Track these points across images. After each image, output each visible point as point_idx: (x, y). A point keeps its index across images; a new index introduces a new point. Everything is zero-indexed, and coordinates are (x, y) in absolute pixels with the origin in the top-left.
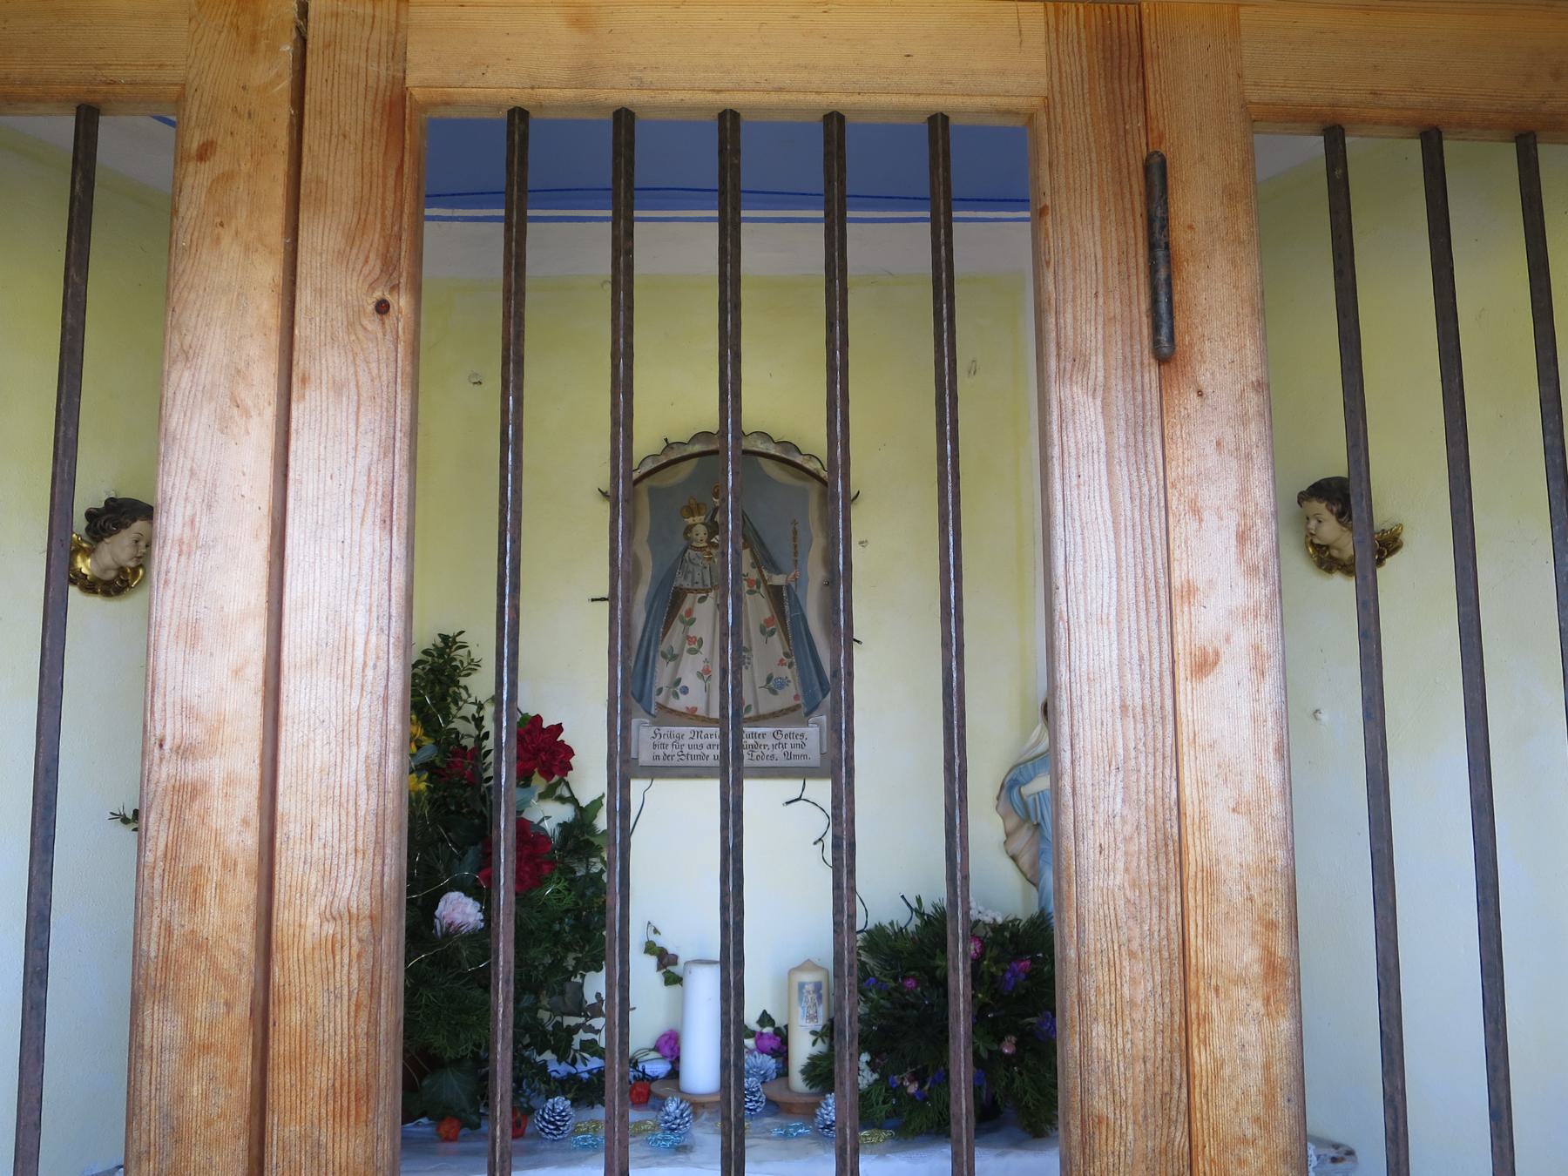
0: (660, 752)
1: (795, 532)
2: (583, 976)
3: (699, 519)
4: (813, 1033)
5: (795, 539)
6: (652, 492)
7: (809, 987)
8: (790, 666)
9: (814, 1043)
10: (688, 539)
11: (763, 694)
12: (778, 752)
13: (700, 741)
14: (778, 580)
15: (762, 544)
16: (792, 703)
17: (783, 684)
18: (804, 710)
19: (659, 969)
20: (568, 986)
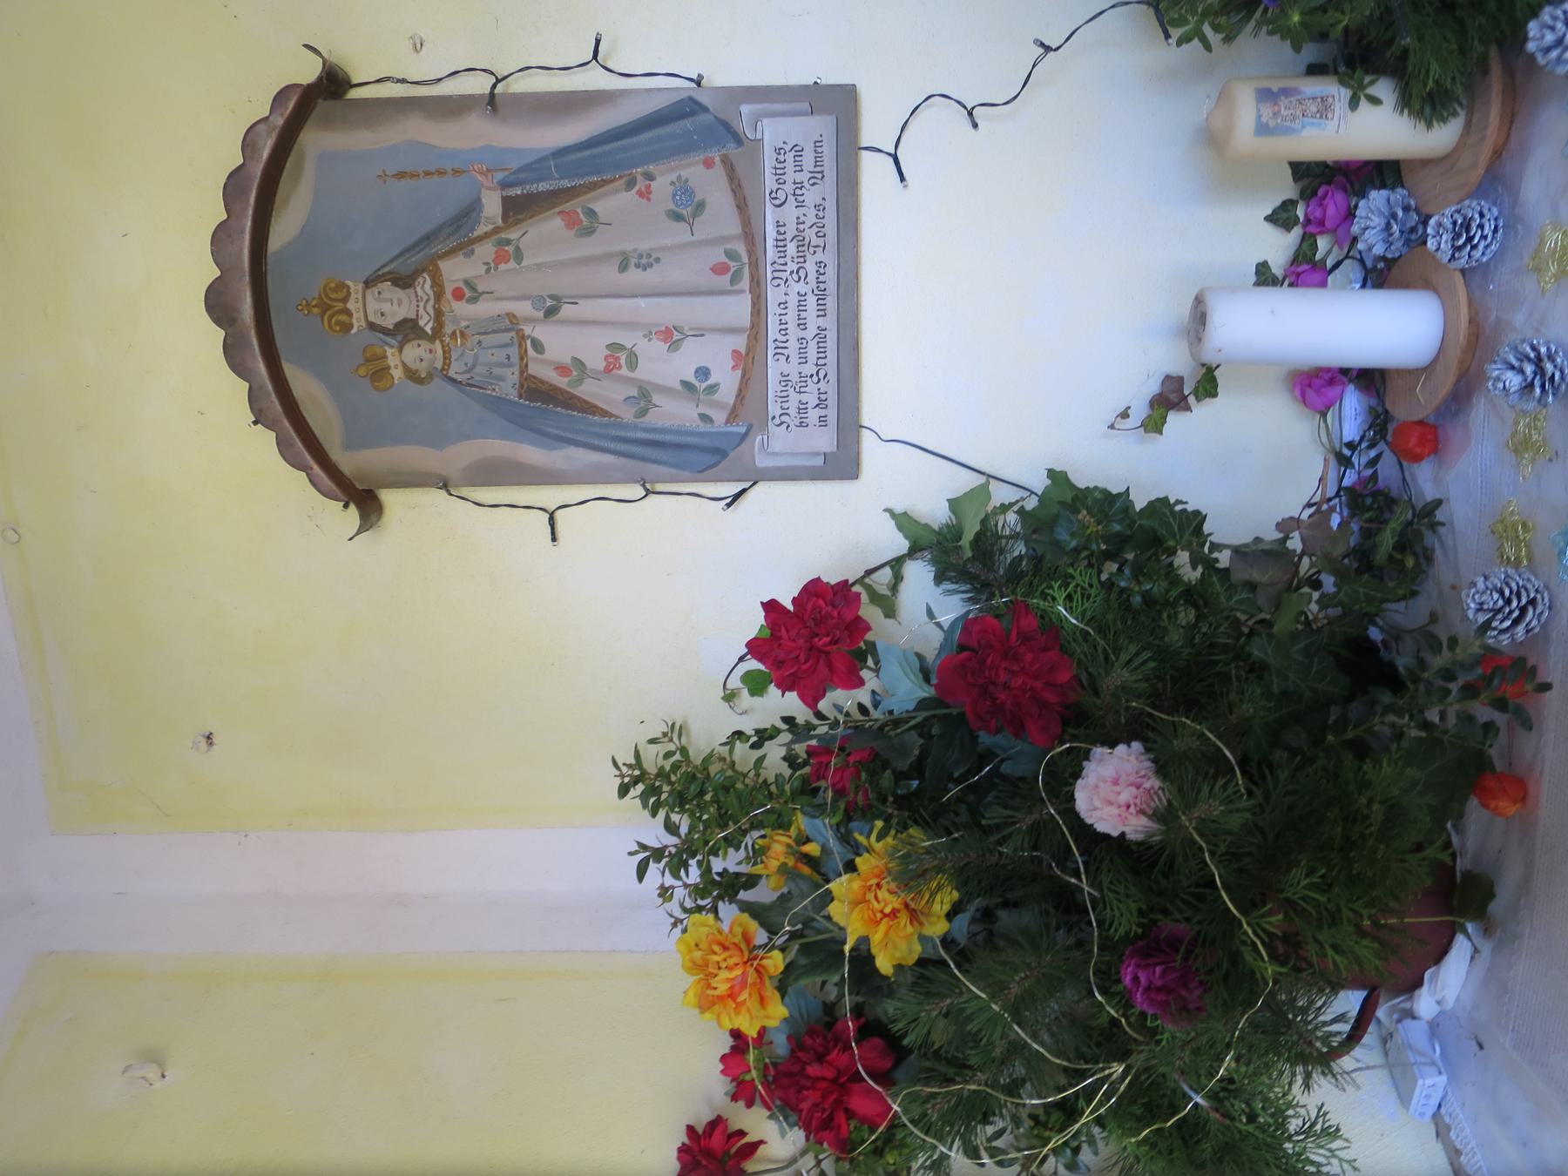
0: (813, 415)
1: (401, 175)
2: (1215, 547)
3: (393, 359)
4: (1354, 104)
5: (414, 176)
6: (351, 445)
7: (1267, 111)
8: (650, 177)
9: (1375, 101)
10: (430, 377)
11: (706, 227)
12: (811, 196)
13: (793, 345)
14: (492, 205)
15: (428, 238)
16: (719, 170)
17: (684, 191)
18: (731, 149)
19: (1188, 409)
20: (1238, 576)
